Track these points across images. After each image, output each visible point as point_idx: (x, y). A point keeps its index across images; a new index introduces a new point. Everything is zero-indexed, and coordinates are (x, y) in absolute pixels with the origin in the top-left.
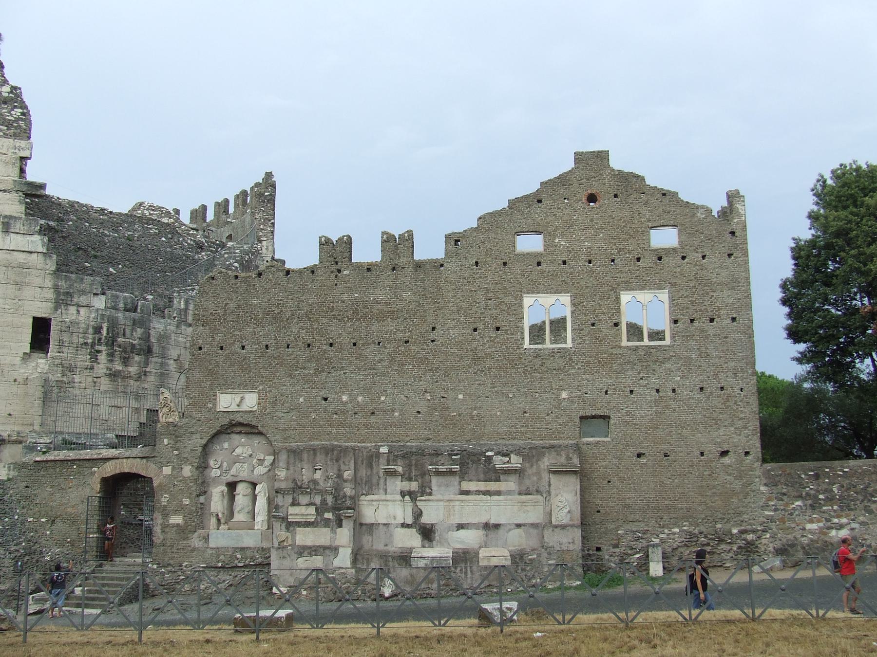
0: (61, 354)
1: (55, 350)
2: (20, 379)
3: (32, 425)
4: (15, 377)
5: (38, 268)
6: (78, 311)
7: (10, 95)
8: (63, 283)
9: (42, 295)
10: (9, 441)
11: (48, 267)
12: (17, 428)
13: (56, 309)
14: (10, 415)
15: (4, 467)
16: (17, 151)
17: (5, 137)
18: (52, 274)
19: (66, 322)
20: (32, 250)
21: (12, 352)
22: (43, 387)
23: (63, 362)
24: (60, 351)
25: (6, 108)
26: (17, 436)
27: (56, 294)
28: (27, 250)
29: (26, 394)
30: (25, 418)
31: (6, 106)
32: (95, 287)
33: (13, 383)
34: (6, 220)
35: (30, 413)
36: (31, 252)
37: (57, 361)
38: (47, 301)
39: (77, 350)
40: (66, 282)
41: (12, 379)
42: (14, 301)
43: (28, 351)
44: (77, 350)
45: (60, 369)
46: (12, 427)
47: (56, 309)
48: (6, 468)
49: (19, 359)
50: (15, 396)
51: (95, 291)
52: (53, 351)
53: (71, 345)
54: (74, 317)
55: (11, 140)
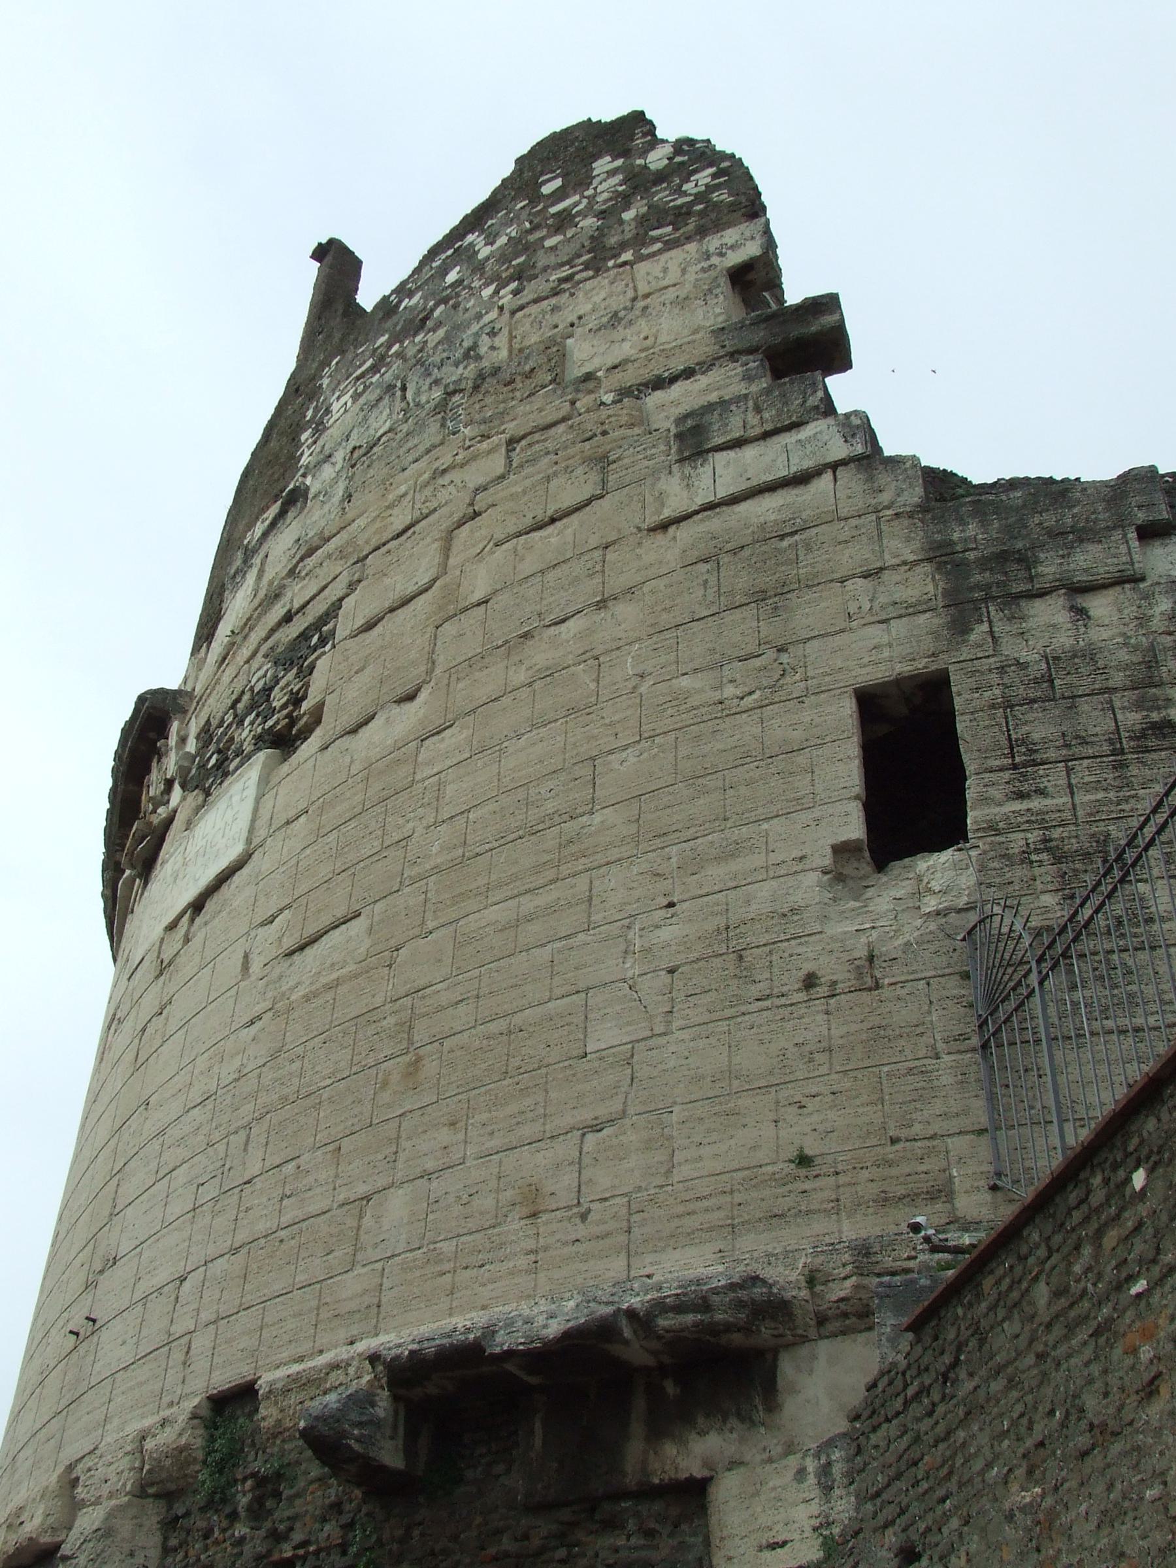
0: (1036, 803)
1: (996, 793)
2: (833, 969)
3: (942, 1192)
4: (808, 967)
5: (843, 513)
6: (1081, 613)
7: (678, 159)
8: (972, 529)
9: (883, 599)
10: (822, 1320)
11: (885, 497)
12: (851, 1230)
13: (960, 627)
14: (803, 1160)
15: (801, 1473)
16: (715, 260)
17: (670, 249)
18: (911, 515)
19: (1022, 666)
20: (808, 464)
21: (774, 858)
22: (966, 976)
23: (1056, 833)
24: (1025, 788)
25: (665, 189)
26: (859, 1271)
27: (947, 574)
28: (783, 473)
29: (879, 1035)
30: (890, 1164)
31: (664, 185)
32: (1134, 501)
33: (802, 996)
34: (690, 423)
35: (917, 1128)
36: (802, 479)
37: (1017, 841)
38: (911, 610)
39: (1120, 766)
40: (984, 524)
41: (792, 982)
42: (757, 662)
43: (854, 828)
44: (1120, 766)
45: (1046, 871)
46: (819, 1226)
47: (960, 627)
48: (812, 1480)
49: (813, 878)
50: (820, 1058)
51: (1141, 516)
52: (985, 800)
53: (1078, 750)
54: (1064, 641)
55: (692, 247)
